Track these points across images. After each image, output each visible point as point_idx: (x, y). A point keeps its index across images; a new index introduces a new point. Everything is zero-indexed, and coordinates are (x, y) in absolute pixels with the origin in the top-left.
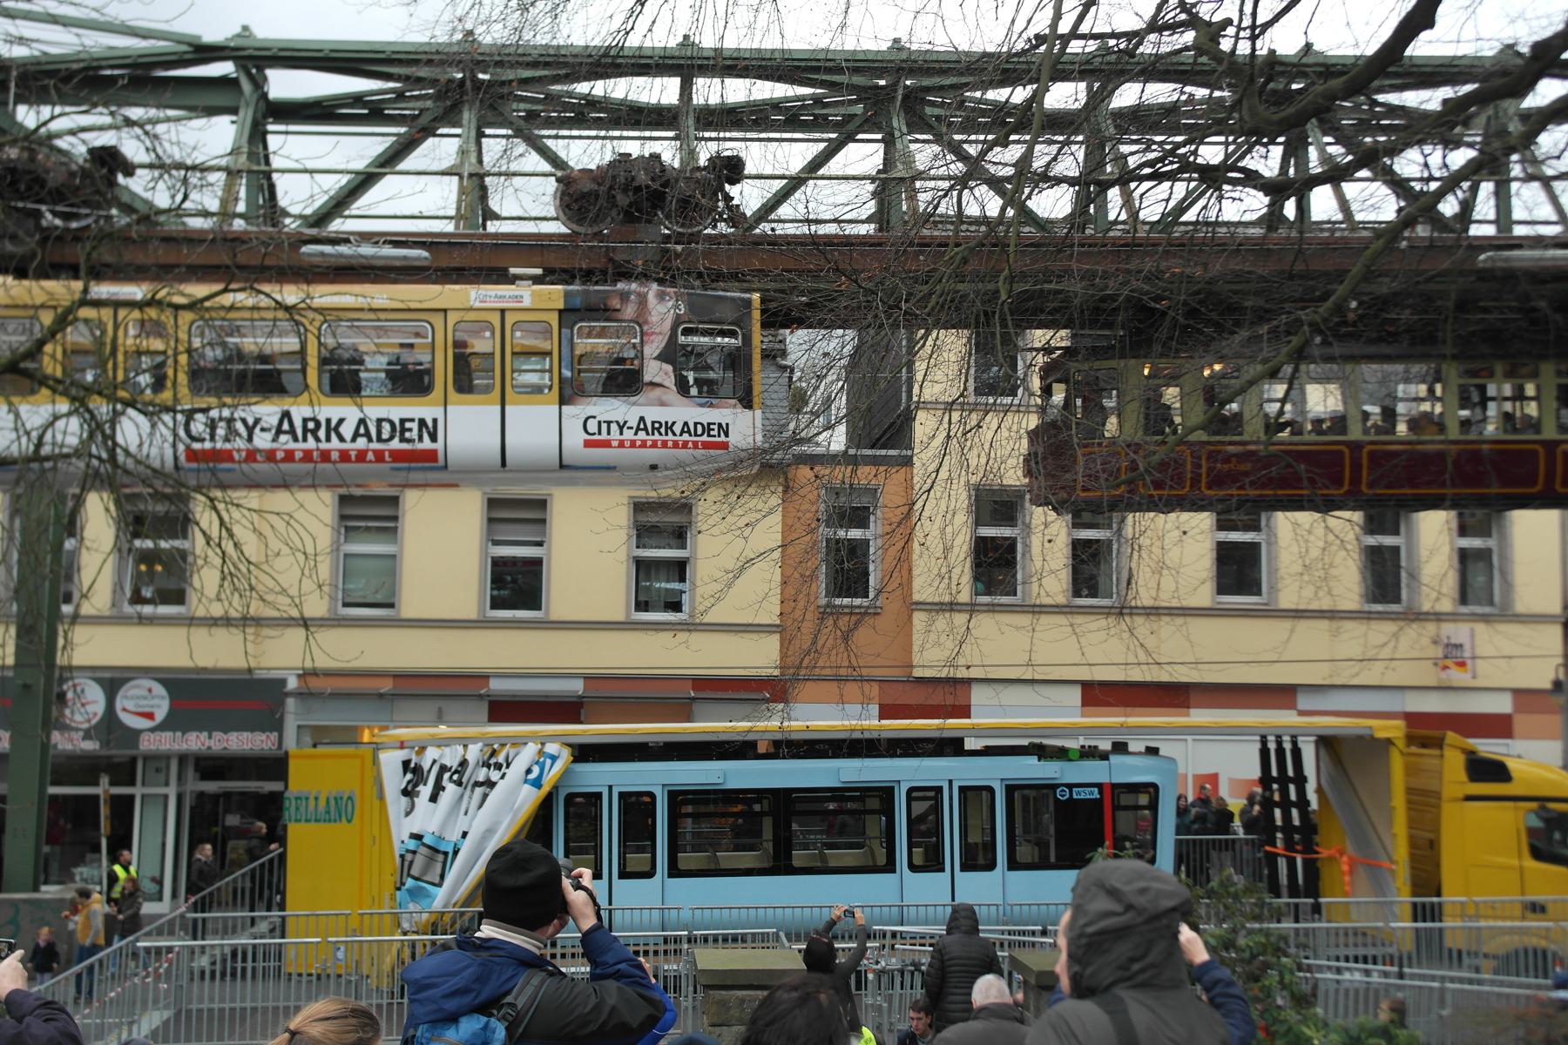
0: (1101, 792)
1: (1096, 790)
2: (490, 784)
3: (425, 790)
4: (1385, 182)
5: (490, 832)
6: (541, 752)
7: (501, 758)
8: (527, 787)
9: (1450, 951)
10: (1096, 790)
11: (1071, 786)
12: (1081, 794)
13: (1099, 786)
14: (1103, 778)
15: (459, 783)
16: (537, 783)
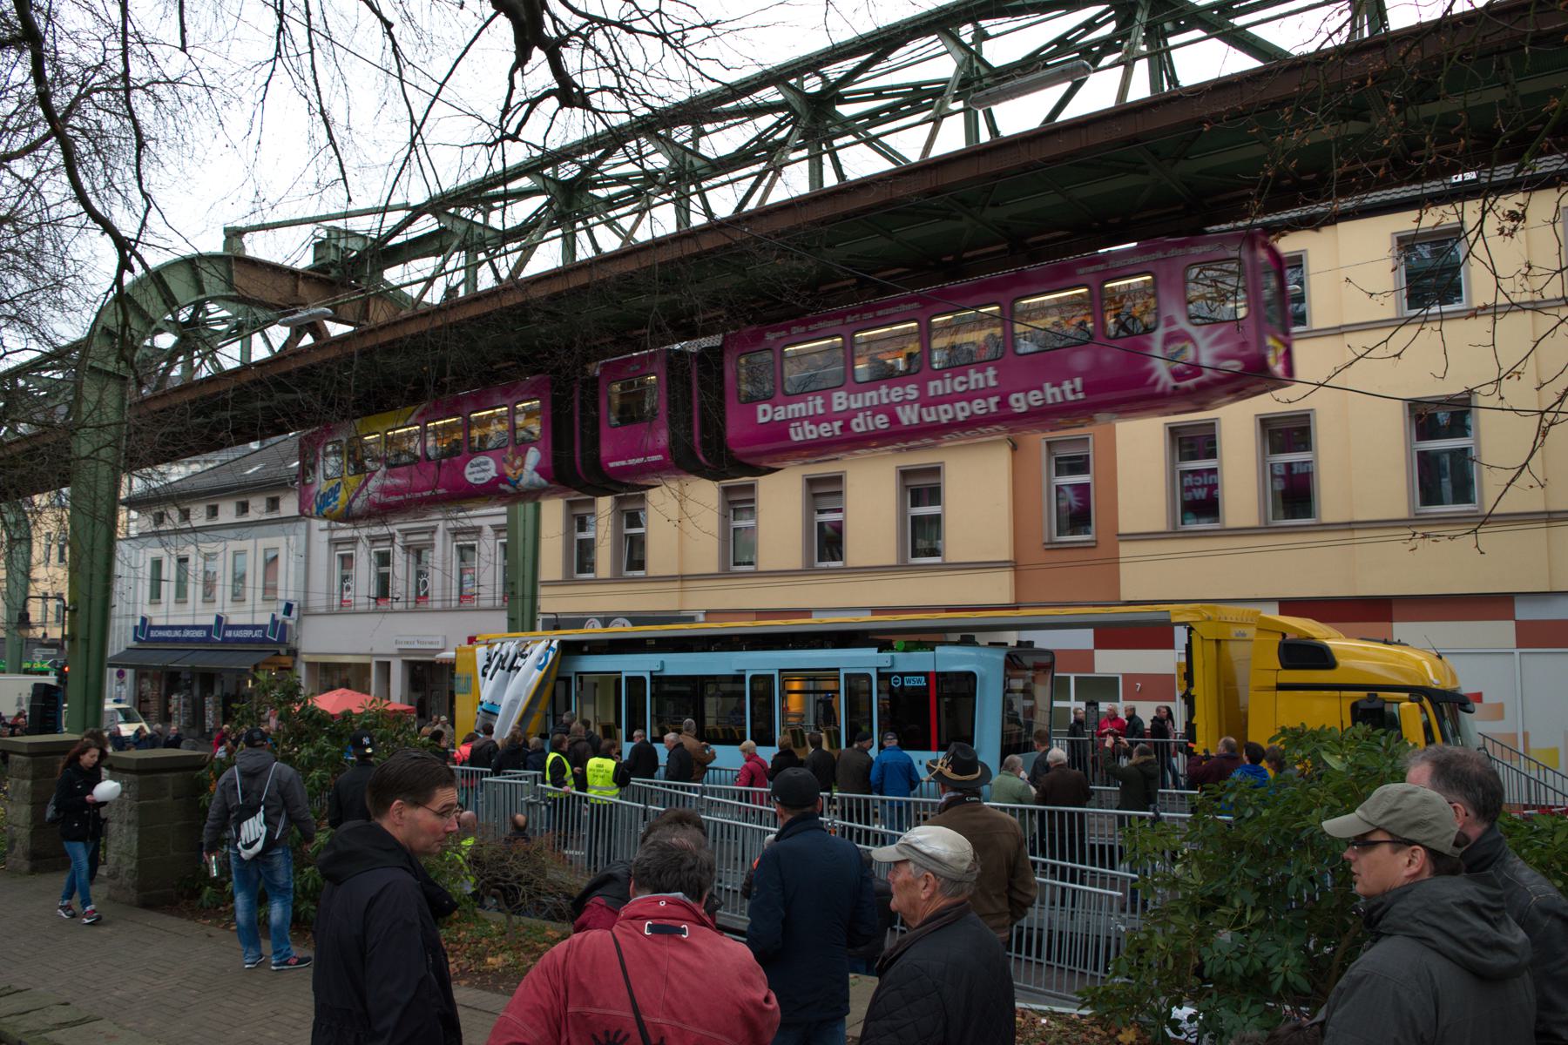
0: (926, 681)
1: (923, 678)
2: (518, 669)
3: (489, 673)
4: (1219, 37)
5: (514, 702)
6: (549, 647)
7: (527, 651)
8: (537, 671)
9: (1092, 846)
10: (923, 678)
11: (902, 675)
12: (910, 682)
13: (925, 674)
14: (929, 668)
15: (503, 668)
16: (540, 668)
